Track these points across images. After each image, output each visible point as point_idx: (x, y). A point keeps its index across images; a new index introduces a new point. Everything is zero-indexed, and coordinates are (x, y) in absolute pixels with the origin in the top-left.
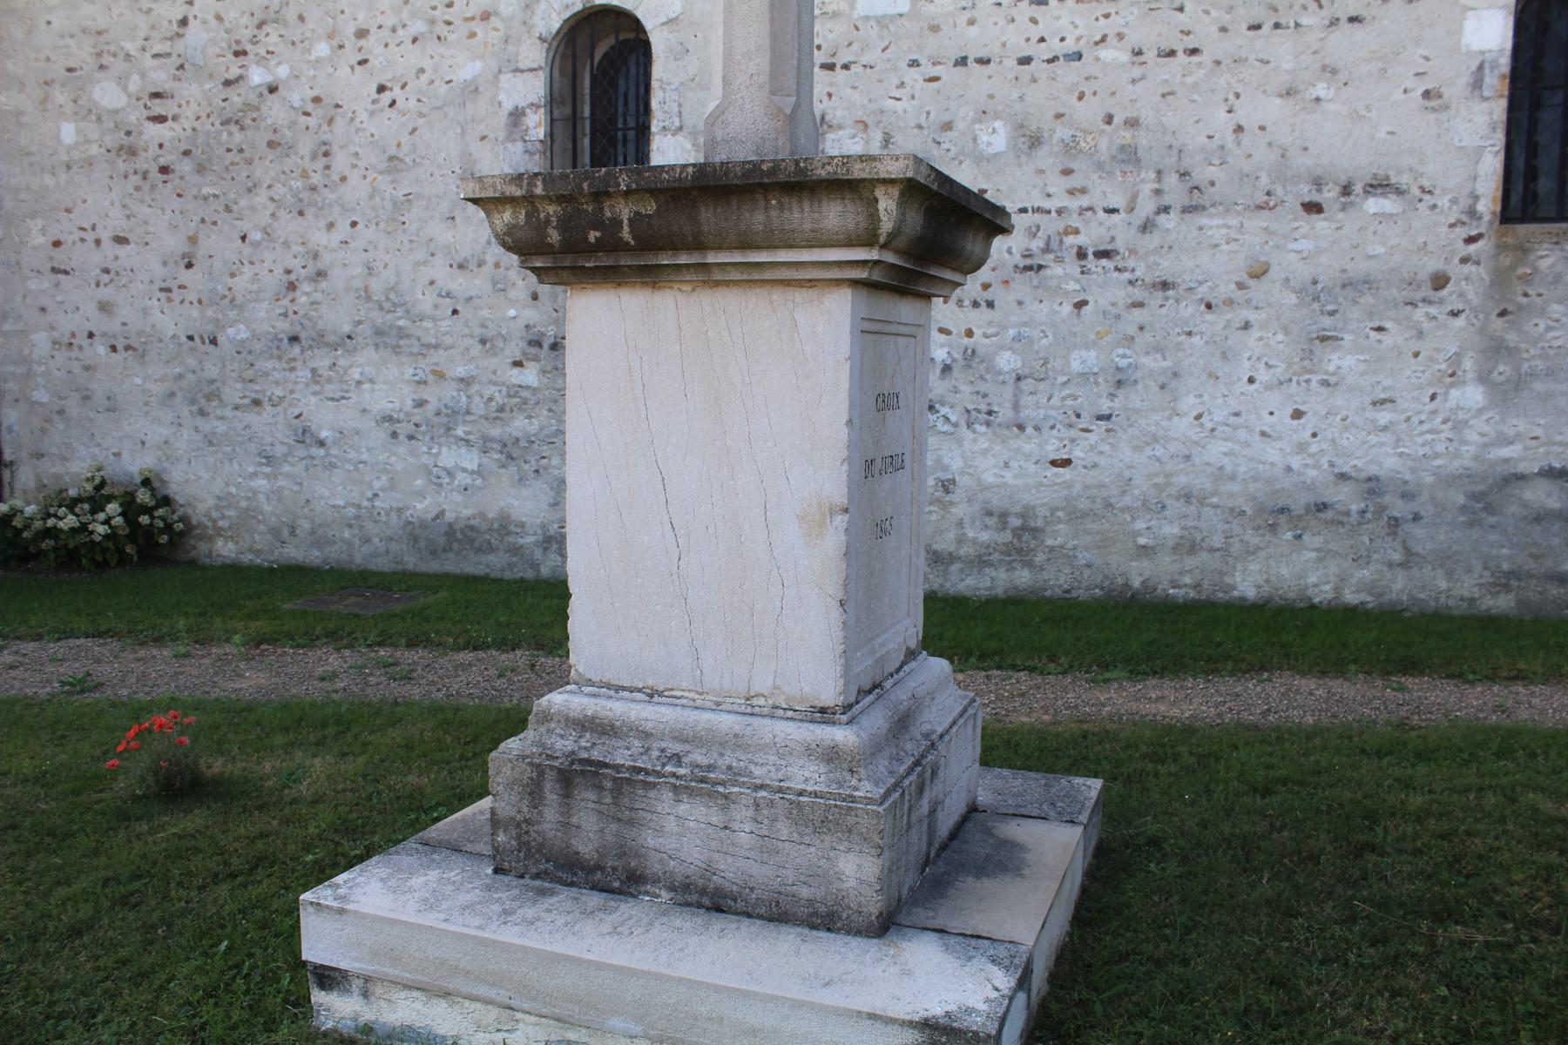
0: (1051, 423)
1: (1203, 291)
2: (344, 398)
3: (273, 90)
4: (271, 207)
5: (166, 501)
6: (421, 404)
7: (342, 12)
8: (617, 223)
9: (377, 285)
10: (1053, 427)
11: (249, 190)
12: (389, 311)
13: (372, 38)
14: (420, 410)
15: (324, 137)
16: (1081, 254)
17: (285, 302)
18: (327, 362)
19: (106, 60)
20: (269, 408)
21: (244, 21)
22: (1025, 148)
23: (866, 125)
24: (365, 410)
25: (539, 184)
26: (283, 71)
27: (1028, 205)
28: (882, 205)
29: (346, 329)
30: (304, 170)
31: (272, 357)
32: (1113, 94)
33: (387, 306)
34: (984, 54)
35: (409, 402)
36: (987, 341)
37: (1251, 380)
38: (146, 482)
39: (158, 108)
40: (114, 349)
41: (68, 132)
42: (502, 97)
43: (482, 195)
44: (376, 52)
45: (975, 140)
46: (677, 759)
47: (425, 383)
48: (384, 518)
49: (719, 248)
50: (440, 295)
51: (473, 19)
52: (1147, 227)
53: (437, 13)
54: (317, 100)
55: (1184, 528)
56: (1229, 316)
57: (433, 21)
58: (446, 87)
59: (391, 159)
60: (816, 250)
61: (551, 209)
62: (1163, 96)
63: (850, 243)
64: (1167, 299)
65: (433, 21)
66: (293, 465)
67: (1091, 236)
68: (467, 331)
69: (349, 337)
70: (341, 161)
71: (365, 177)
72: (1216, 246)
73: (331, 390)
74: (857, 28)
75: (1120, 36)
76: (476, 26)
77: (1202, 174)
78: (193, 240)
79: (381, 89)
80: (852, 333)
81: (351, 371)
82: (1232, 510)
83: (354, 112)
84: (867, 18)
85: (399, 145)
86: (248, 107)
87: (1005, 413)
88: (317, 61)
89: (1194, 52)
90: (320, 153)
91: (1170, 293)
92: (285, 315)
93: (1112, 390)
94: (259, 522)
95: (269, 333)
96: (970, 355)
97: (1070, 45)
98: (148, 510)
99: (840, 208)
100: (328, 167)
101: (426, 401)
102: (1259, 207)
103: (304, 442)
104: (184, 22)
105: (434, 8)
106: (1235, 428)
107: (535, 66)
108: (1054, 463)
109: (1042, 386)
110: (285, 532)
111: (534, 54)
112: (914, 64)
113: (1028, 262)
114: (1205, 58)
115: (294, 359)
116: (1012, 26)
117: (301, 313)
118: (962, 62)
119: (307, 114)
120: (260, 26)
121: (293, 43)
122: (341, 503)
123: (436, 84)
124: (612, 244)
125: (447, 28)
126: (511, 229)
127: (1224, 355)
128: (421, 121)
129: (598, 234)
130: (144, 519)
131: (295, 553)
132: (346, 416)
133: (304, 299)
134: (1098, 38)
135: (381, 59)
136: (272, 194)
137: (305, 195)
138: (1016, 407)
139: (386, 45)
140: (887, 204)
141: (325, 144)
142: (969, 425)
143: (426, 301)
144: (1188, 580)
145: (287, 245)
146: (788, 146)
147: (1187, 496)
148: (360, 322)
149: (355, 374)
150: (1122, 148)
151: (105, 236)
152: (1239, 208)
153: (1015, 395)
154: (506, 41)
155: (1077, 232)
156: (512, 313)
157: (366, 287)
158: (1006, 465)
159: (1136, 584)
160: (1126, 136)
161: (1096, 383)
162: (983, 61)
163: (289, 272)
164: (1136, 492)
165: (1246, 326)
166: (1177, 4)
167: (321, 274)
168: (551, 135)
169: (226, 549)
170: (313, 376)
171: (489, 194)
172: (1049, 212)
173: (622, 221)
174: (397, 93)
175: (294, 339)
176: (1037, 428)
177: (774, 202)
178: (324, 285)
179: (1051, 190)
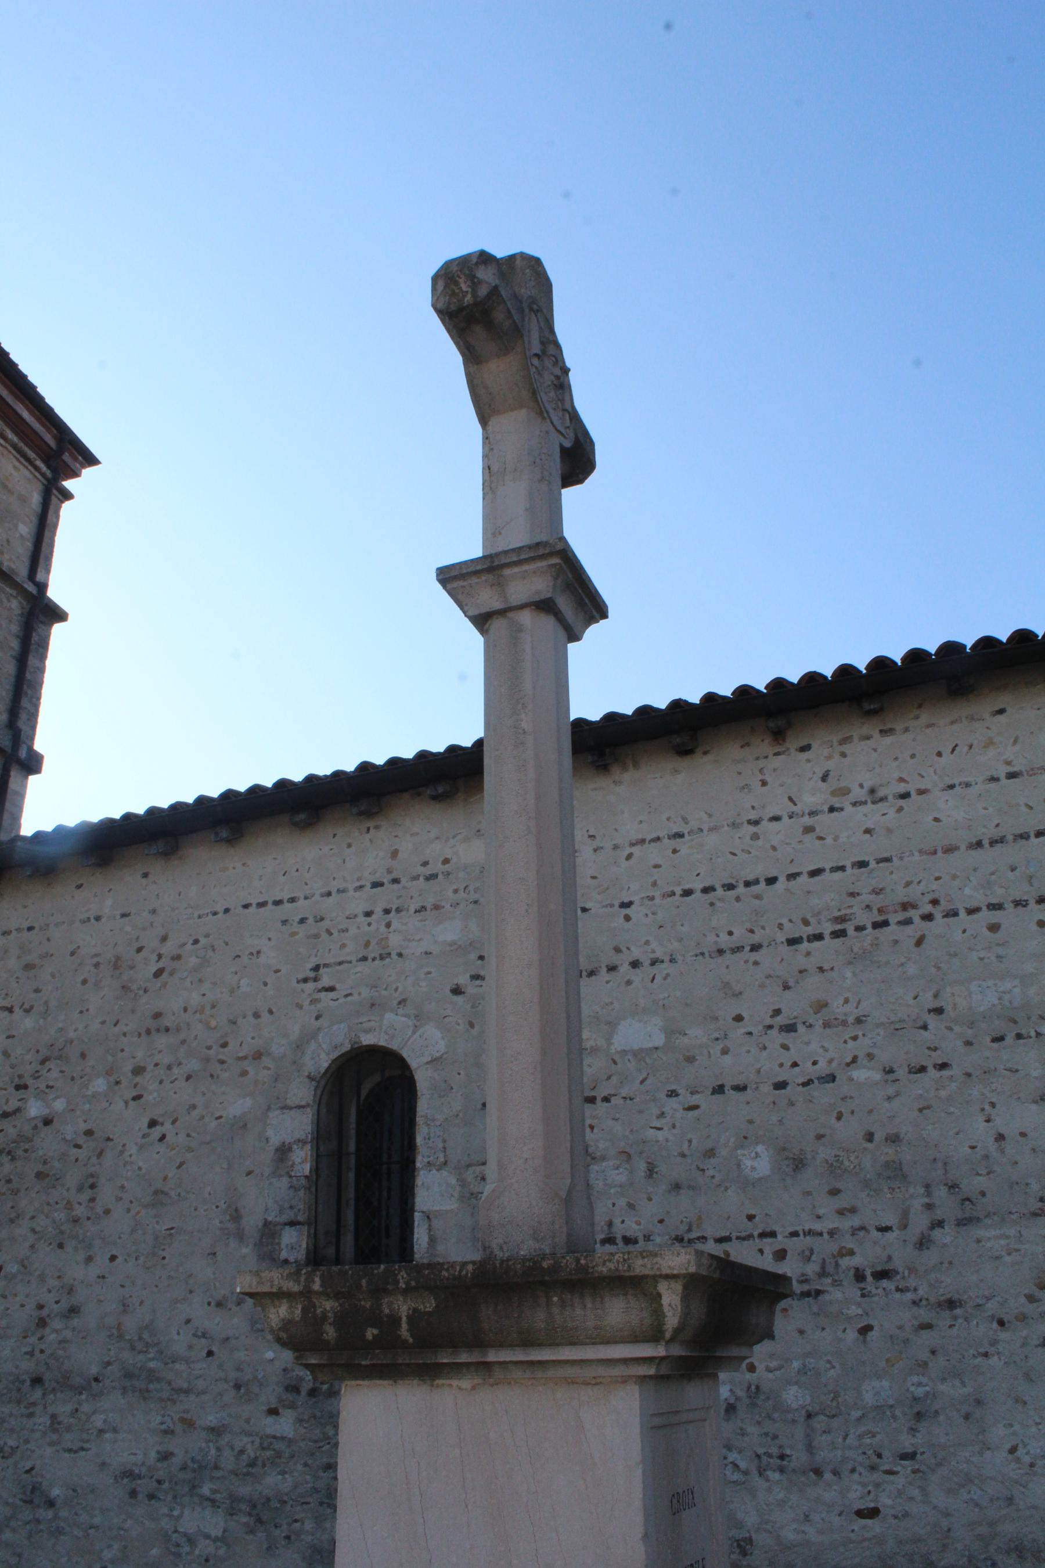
0: (850, 1466)
1: (992, 1306)
2: (82, 1449)
3: (47, 1122)
6: (165, 1456)
7: (122, 1050)
8: (395, 1320)
10: (853, 1470)
11: (12, 1221)
12: (140, 1352)
13: (148, 1075)
14: (165, 1464)
16: (859, 1276)
17: (33, 1340)
18: (69, 1408)
21: (29, 1057)
23: (629, 1155)
24: (103, 1464)
25: (317, 1280)
26: (59, 1105)
27: (799, 1228)
28: (666, 1300)
29: (94, 1370)
30: (69, 1202)
31: (10, 1401)
32: (871, 1111)
33: (139, 1346)
34: (739, 1080)
35: (153, 1455)
36: (770, 1375)
42: (270, 1133)
43: (259, 1290)
44: (151, 1088)
45: (739, 1166)
47: (172, 1432)
49: (501, 1345)
50: (195, 1335)
51: (245, 1058)
52: (923, 1243)
53: (211, 1052)
54: (89, 1133)
56: (1024, 1333)
58: (215, 1123)
59: (156, 1193)
60: (601, 1347)
61: (328, 1305)
62: (920, 1110)
63: (635, 1339)
64: (955, 1318)
65: (207, 1060)
69: (96, 1380)
70: (106, 1194)
71: (129, 1210)
72: (997, 1258)
74: (615, 1063)
76: (246, 1065)
79: (153, 1124)
80: (641, 1432)
83: (124, 1145)
85: (165, 1179)
86: (22, 1138)
87: (799, 1457)
88: (94, 1095)
89: (943, 1066)
91: (958, 1311)
92: (31, 1354)
96: (755, 1392)
97: (822, 1068)
100: (92, 1200)
101: (172, 1454)
102: (1035, 1215)
105: (209, 1048)
107: (303, 1103)
108: (860, 1514)
109: (835, 1423)
111: (302, 1092)
112: (673, 1094)
114: (955, 1071)
115: (34, 1404)
116: (764, 1054)
117: (48, 1352)
118: (719, 1089)
119: (78, 1146)
120: (43, 1062)
121: (73, 1079)
123: (207, 1119)
124: (389, 1341)
126: (287, 1324)
127: (1028, 1377)
129: (375, 1331)
133: (53, 1336)
134: (849, 1059)
135: (155, 1094)
138: (810, 1448)
139: (161, 1082)
140: (671, 1298)
142: (761, 1473)
146: (565, 1229)
148: (109, 1363)
149: (98, 1421)
150: (887, 1165)
152: (1014, 1217)
154: (276, 1080)
155: (851, 1253)
157: (119, 1325)
158: (807, 1518)
160: (889, 1152)
161: (894, 1417)
162: (741, 1088)
163: (41, 1307)
166: (921, 1023)
167: (74, 1310)
168: (316, 1170)
170: (52, 1424)
171: (266, 1288)
172: (821, 1234)
173: (400, 1318)
174: (167, 1127)
175: (37, 1381)
176: (836, 1473)
177: (555, 1299)
178: (75, 1322)
179: (821, 1212)
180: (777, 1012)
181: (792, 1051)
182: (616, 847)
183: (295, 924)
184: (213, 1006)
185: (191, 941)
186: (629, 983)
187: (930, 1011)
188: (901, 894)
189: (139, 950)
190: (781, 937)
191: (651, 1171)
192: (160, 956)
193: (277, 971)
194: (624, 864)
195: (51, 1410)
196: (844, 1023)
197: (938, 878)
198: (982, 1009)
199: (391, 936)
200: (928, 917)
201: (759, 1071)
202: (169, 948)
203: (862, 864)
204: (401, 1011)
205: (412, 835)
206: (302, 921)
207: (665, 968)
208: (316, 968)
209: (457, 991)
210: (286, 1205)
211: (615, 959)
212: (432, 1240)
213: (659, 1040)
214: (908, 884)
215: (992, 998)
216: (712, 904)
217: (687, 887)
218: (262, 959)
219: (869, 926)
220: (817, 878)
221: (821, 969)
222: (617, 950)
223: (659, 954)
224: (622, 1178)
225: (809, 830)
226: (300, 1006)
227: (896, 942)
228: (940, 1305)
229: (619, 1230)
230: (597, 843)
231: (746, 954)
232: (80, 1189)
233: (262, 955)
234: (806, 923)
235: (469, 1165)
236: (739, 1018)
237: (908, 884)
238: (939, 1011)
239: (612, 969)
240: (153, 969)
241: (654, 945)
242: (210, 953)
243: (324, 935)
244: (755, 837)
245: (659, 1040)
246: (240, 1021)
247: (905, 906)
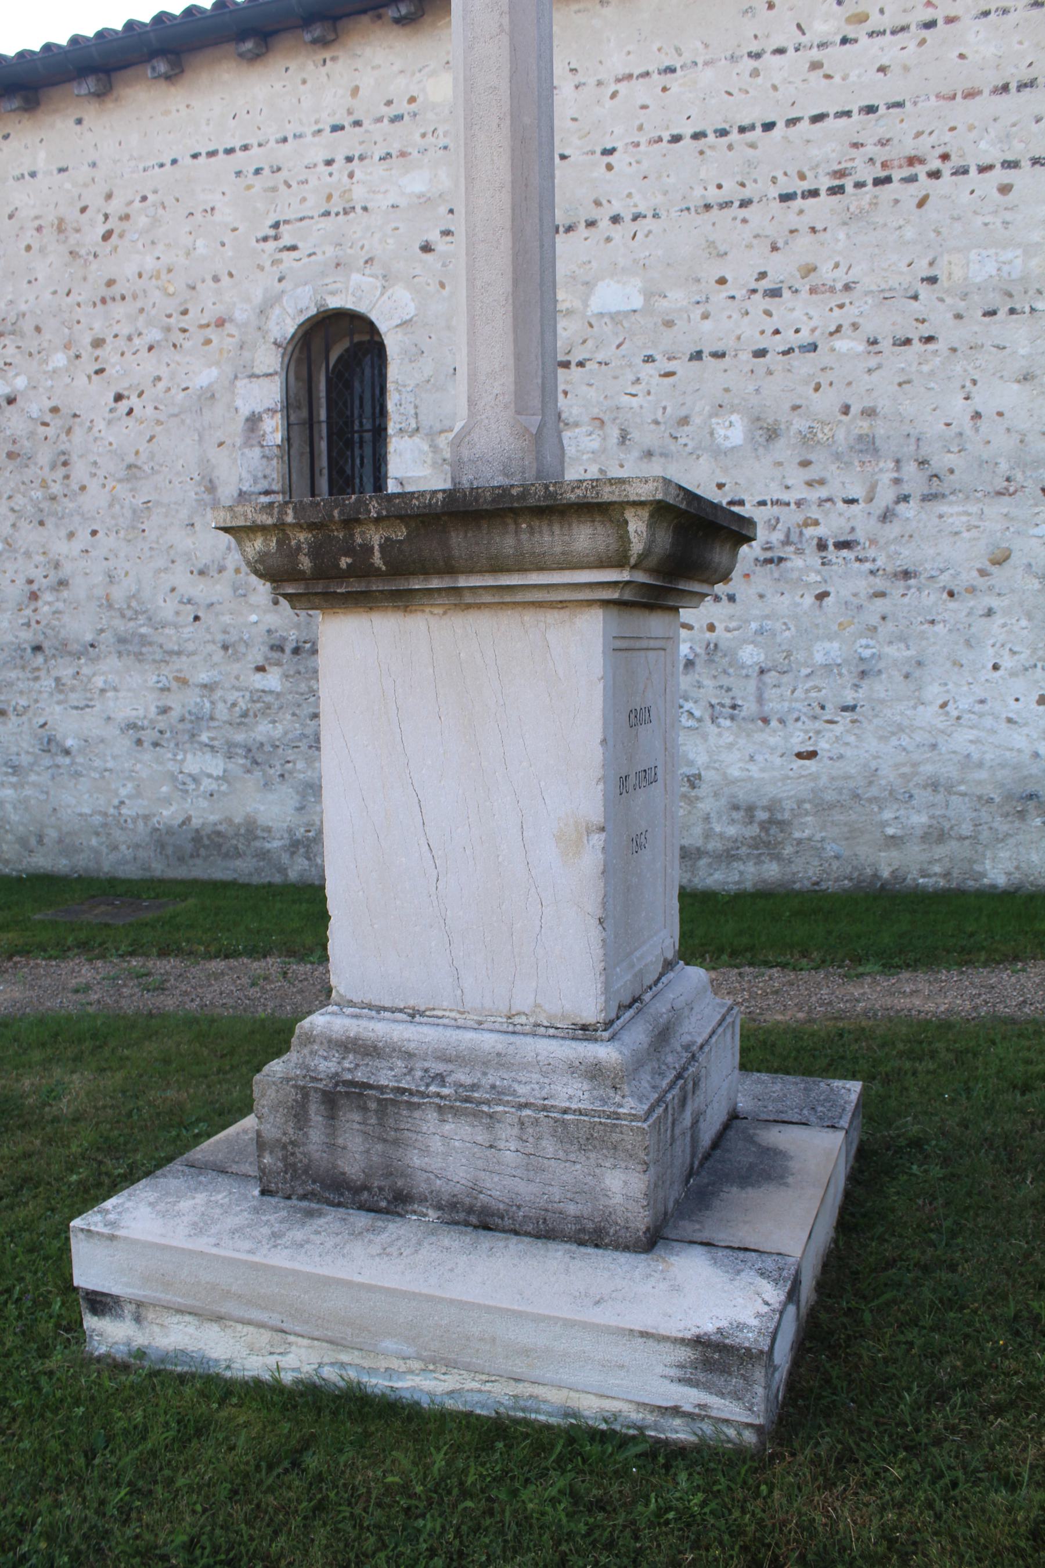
0: (795, 716)
1: (944, 579)
2: (88, 706)
4: (12, 517)
6: (164, 711)
7: (78, 322)
8: (368, 549)
9: (118, 594)
10: (797, 720)
12: (131, 619)
13: (108, 347)
14: (164, 717)
15: (63, 447)
16: (822, 546)
17: (28, 612)
18: (70, 671)
20: (13, 718)
22: (762, 440)
23: (603, 422)
24: (109, 718)
25: (290, 512)
26: (21, 382)
27: (768, 498)
28: (632, 527)
29: (89, 637)
30: (44, 481)
31: (15, 667)
32: (849, 384)
33: (129, 613)
34: (718, 347)
35: (153, 710)
36: (729, 635)
37: (996, 667)
42: (239, 403)
43: (234, 524)
44: (113, 360)
45: (712, 434)
46: (441, 1078)
47: (169, 689)
48: (131, 826)
49: (471, 571)
50: (181, 602)
51: (208, 325)
52: (886, 516)
53: (172, 320)
54: (55, 410)
55: (932, 817)
56: (972, 603)
57: (168, 329)
58: (183, 394)
59: (130, 467)
60: (567, 572)
61: (302, 536)
62: (900, 384)
63: (601, 564)
64: (909, 588)
65: (168, 329)
66: (39, 774)
67: (830, 528)
68: (209, 637)
69: (92, 646)
70: (80, 471)
71: (104, 486)
72: (957, 533)
73: (75, 698)
74: (591, 326)
75: (855, 326)
76: (211, 333)
77: (941, 461)
79: (118, 398)
80: (604, 652)
81: (94, 679)
82: (980, 798)
83: (92, 421)
84: (601, 315)
85: (137, 453)
87: (749, 707)
89: (930, 339)
90: (59, 463)
91: (912, 582)
92: (28, 625)
93: (856, 681)
94: (7, 831)
95: (12, 643)
96: (713, 649)
97: (805, 337)
99: (590, 531)
100: (67, 477)
101: (170, 708)
102: (999, 494)
103: (49, 751)
105: (169, 316)
106: (981, 715)
107: (271, 371)
108: (799, 755)
109: (785, 679)
110: (33, 841)
111: (270, 360)
112: (649, 359)
113: (769, 555)
114: (940, 346)
115: (38, 669)
116: (746, 319)
117: (44, 623)
118: (697, 356)
119: (45, 424)
121: (30, 354)
122: (86, 810)
123: (173, 391)
124: (363, 570)
125: (182, 335)
126: (263, 557)
127: (968, 643)
128: (159, 428)
129: (349, 560)
131: (42, 861)
132: (91, 724)
133: (46, 608)
134: (833, 328)
135: (118, 368)
136: (12, 505)
137: (45, 505)
138: (760, 700)
139: (122, 354)
140: (637, 526)
141: (64, 453)
143: (167, 609)
144: (937, 869)
145: (28, 554)
146: (535, 465)
147: (934, 785)
148: (102, 631)
149: (99, 682)
150: (860, 438)
153: (759, 689)
154: (241, 347)
155: (816, 523)
156: (254, 618)
158: (752, 758)
159: (886, 874)
160: (864, 426)
161: (840, 674)
162: (719, 355)
163: (30, 582)
165: (990, 613)
166: (911, 293)
167: (63, 583)
168: (288, 439)
170: (57, 685)
171: (241, 522)
172: (788, 504)
173: (373, 547)
174: (134, 401)
175: (37, 649)
176: (781, 721)
177: (524, 526)
178: (65, 594)
179: (790, 483)
180: (763, 275)
181: (775, 317)
182: (600, 83)
183: (250, 175)
184: (170, 271)
185: (138, 198)
186: (608, 240)
187: (923, 280)
188: (910, 147)
189: (83, 210)
190: (774, 192)
191: (624, 437)
192: (106, 217)
193: (234, 230)
194: (608, 103)
195: (55, 673)
196: (832, 290)
197: (952, 129)
198: (978, 280)
199: (354, 187)
200: (935, 175)
201: (739, 338)
202: (115, 207)
203: (871, 109)
204: (367, 271)
205: (373, 68)
206: (258, 171)
207: (648, 224)
208: (276, 225)
209: (426, 248)
210: (260, 475)
211: (594, 213)
213: (638, 302)
214: (919, 134)
215: (991, 268)
216: (702, 153)
217: (675, 132)
218: (218, 217)
219: (870, 182)
220: (819, 125)
221: (813, 230)
222: (598, 203)
223: (642, 209)
224: (595, 444)
225: (816, 66)
226: (261, 268)
227: (897, 201)
228: (895, 575)
230: (580, 78)
231: (735, 210)
232: (53, 467)
233: (216, 212)
234: (802, 177)
235: (442, 432)
236: (722, 281)
237: (919, 134)
238: (932, 280)
239: (591, 224)
240: (101, 230)
241: (637, 198)
242: (160, 211)
243: (282, 188)
244: (755, 73)
245: (638, 302)
246: (199, 286)
247: (912, 161)
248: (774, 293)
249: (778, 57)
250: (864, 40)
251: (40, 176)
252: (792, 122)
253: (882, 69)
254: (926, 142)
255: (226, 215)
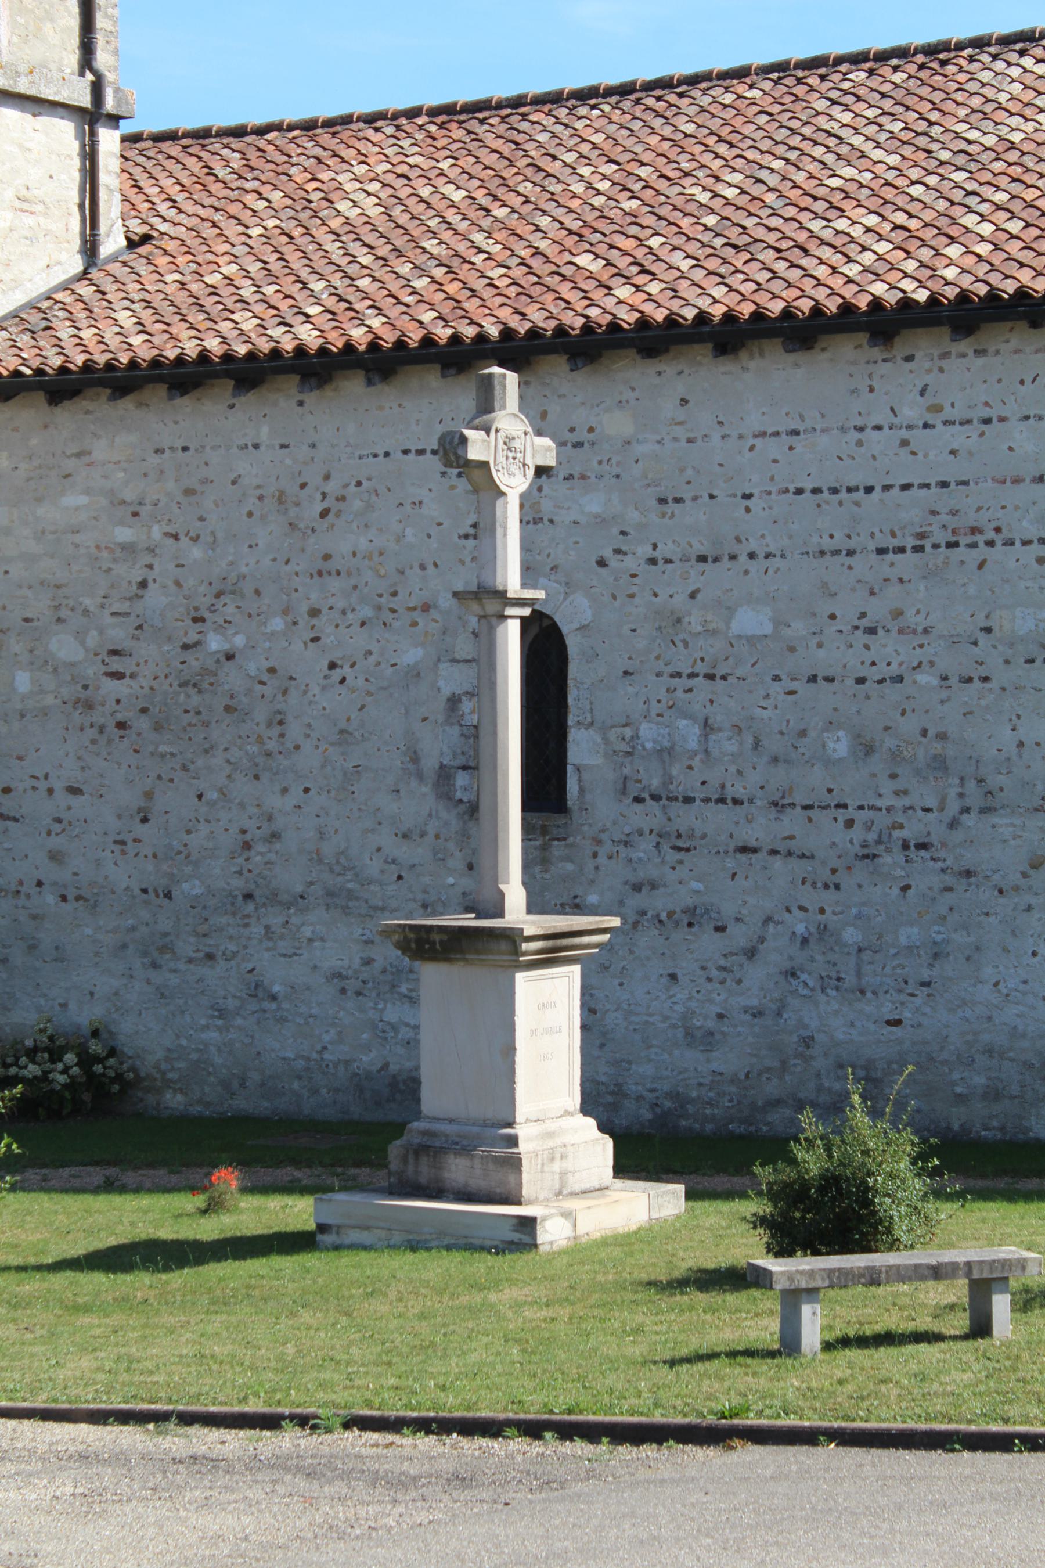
0: (885, 988)
1: (996, 877)
2: (295, 954)
3: (230, 657)
4: (228, 769)
5: (112, 1052)
6: (368, 962)
7: (296, 590)
9: (328, 849)
10: (886, 992)
11: (206, 751)
12: (339, 874)
13: (324, 617)
14: (368, 968)
15: (279, 707)
16: (905, 846)
17: (240, 860)
18: (281, 920)
19: (64, 613)
20: (222, 963)
21: (202, 589)
22: (861, 754)
23: (740, 729)
24: (315, 967)
26: (239, 641)
27: (865, 803)
29: (299, 889)
30: (259, 736)
31: (226, 913)
32: (927, 711)
33: (338, 869)
34: (829, 673)
35: (357, 961)
36: (835, 918)
37: (1034, 954)
38: (95, 1034)
39: (116, 664)
40: (64, 898)
41: (23, 681)
42: (441, 683)
44: (328, 631)
45: (824, 746)
46: (457, 1143)
47: (372, 942)
48: (332, 1071)
50: (386, 862)
51: (414, 609)
52: (953, 824)
53: (383, 600)
54: (272, 670)
55: (989, 1078)
56: (1016, 900)
57: (379, 608)
58: (391, 669)
59: (342, 732)
62: (965, 715)
64: (970, 885)
65: (379, 608)
66: (245, 1018)
67: (910, 832)
68: (410, 896)
69: (302, 897)
70: (294, 731)
71: (317, 747)
72: (1005, 841)
73: (283, 946)
74: (732, 645)
75: (932, 664)
76: (416, 615)
77: (995, 780)
78: (149, 795)
79: (332, 666)
81: (303, 929)
82: (1025, 1063)
84: (740, 637)
85: (349, 719)
86: (205, 672)
87: (850, 980)
88: (273, 634)
89: (986, 679)
90: (275, 722)
91: (972, 880)
92: (240, 873)
93: (931, 961)
94: (210, 1073)
95: (224, 890)
96: (823, 930)
97: (894, 669)
98: (100, 1060)
101: (373, 960)
102: (1037, 810)
103: (256, 996)
104: (143, 584)
105: (380, 596)
106: (1024, 994)
107: (469, 657)
108: (889, 1023)
109: (877, 956)
110: (235, 1084)
112: (776, 678)
113: (866, 851)
114: (993, 685)
115: (248, 916)
116: (851, 651)
117: (257, 871)
118: (813, 679)
120: (218, 596)
121: (250, 616)
122: (291, 1055)
123: (383, 666)
125: (392, 616)
127: (1013, 933)
128: (369, 699)
130: (98, 1068)
131: (242, 1104)
133: (258, 858)
134: (915, 664)
135: (332, 638)
136: (229, 756)
137: (260, 760)
138: (859, 974)
139: (337, 626)
141: (280, 713)
142: (823, 990)
143: (373, 867)
144: (995, 1123)
145: (242, 806)
147: (989, 1051)
148: (312, 883)
149: (307, 932)
150: (935, 757)
151: (58, 786)
152: (1021, 810)
153: (857, 964)
155: (901, 827)
156: (451, 880)
158: (852, 1024)
159: (956, 1127)
160: (937, 747)
161: (919, 955)
162: (830, 680)
163: (244, 832)
164: (952, 1048)
165: (1029, 908)
166: (972, 640)
167: (275, 836)
169: (174, 1101)
170: (267, 933)
172: (880, 810)
174: (346, 670)
175: (248, 896)
176: (874, 993)
178: (278, 846)
179: (882, 791)
180: (863, 615)
181: (872, 651)
182: (741, 437)
184: (381, 554)
185: (354, 483)
186: (746, 572)
187: (982, 629)
188: (971, 519)
189: (303, 486)
190: (872, 546)
191: (757, 744)
192: (324, 496)
193: (439, 524)
194: (748, 455)
195: (264, 921)
196: (914, 632)
197: (1003, 507)
198: (1021, 633)
199: (542, 500)
200: (990, 543)
201: (845, 666)
202: (332, 487)
203: (944, 485)
204: (552, 577)
205: (559, 396)
207: (777, 562)
209: (602, 563)
210: (459, 751)
211: (736, 549)
212: (582, 790)
213: (768, 629)
214: (979, 509)
215: (1030, 624)
216: (819, 505)
217: (799, 486)
219: (943, 544)
220: (906, 493)
221: (901, 580)
222: (738, 540)
223: (772, 549)
224: (731, 747)
225: (905, 443)
226: (462, 562)
227: (963, 562)
228: (960, 873)
229: (730, 792)
230: (725, 430)
231: (842, 558)
232: (269, 724)
234: (893, 535)
235: (612, 727)
236: (833, 617)
237: (979, 509)
238: (988, 630)
239: (733, 557)
240: (319, 507)
241: (768, 539)
242: (374, 498)
244: (860, 443)
245: (768, 629)
246: (408, 572)
247: (974, 530)
248: (872, 631)
249: (877, 432)
250: (940, 426)
251: (263, 448)
252: (887, 488)
253: (953, 452)
254: (981, 519)
255: (432, 509)
